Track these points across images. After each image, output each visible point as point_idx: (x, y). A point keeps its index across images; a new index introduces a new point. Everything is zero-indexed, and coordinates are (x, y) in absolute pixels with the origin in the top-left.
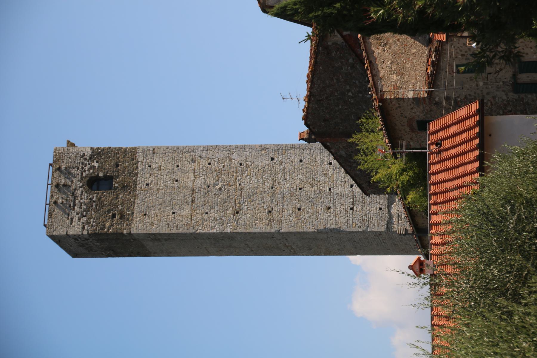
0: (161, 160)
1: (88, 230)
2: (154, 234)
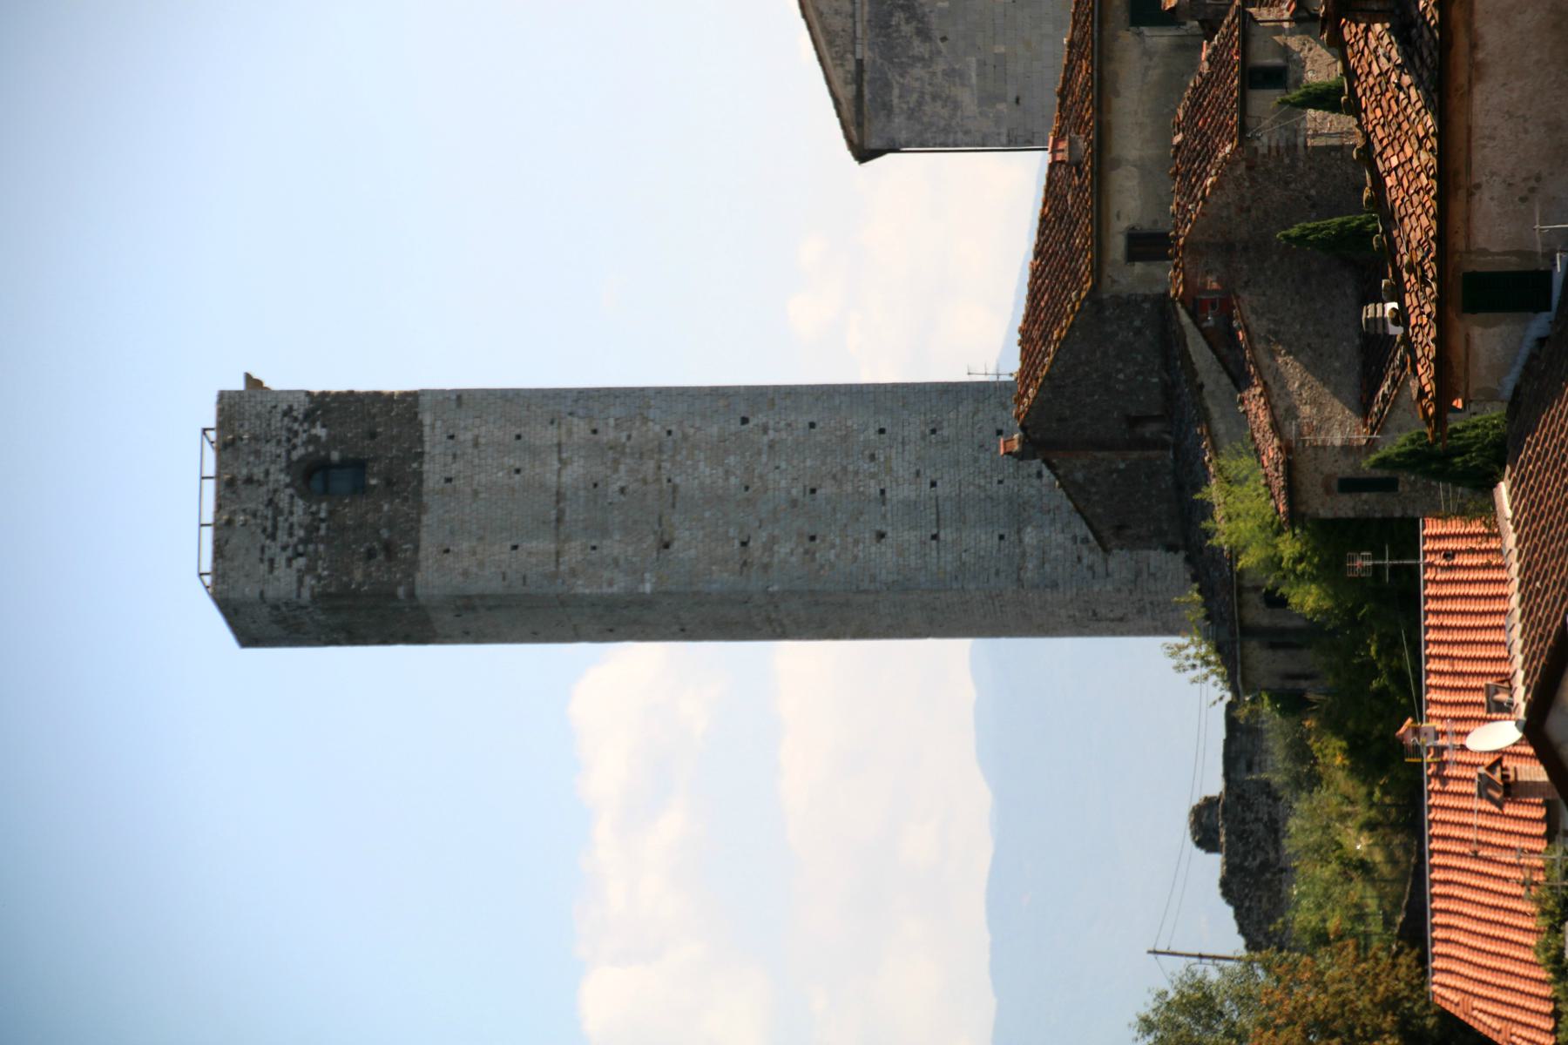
0: (477, 421)
1: (312, 588)
2: (469, 597)
